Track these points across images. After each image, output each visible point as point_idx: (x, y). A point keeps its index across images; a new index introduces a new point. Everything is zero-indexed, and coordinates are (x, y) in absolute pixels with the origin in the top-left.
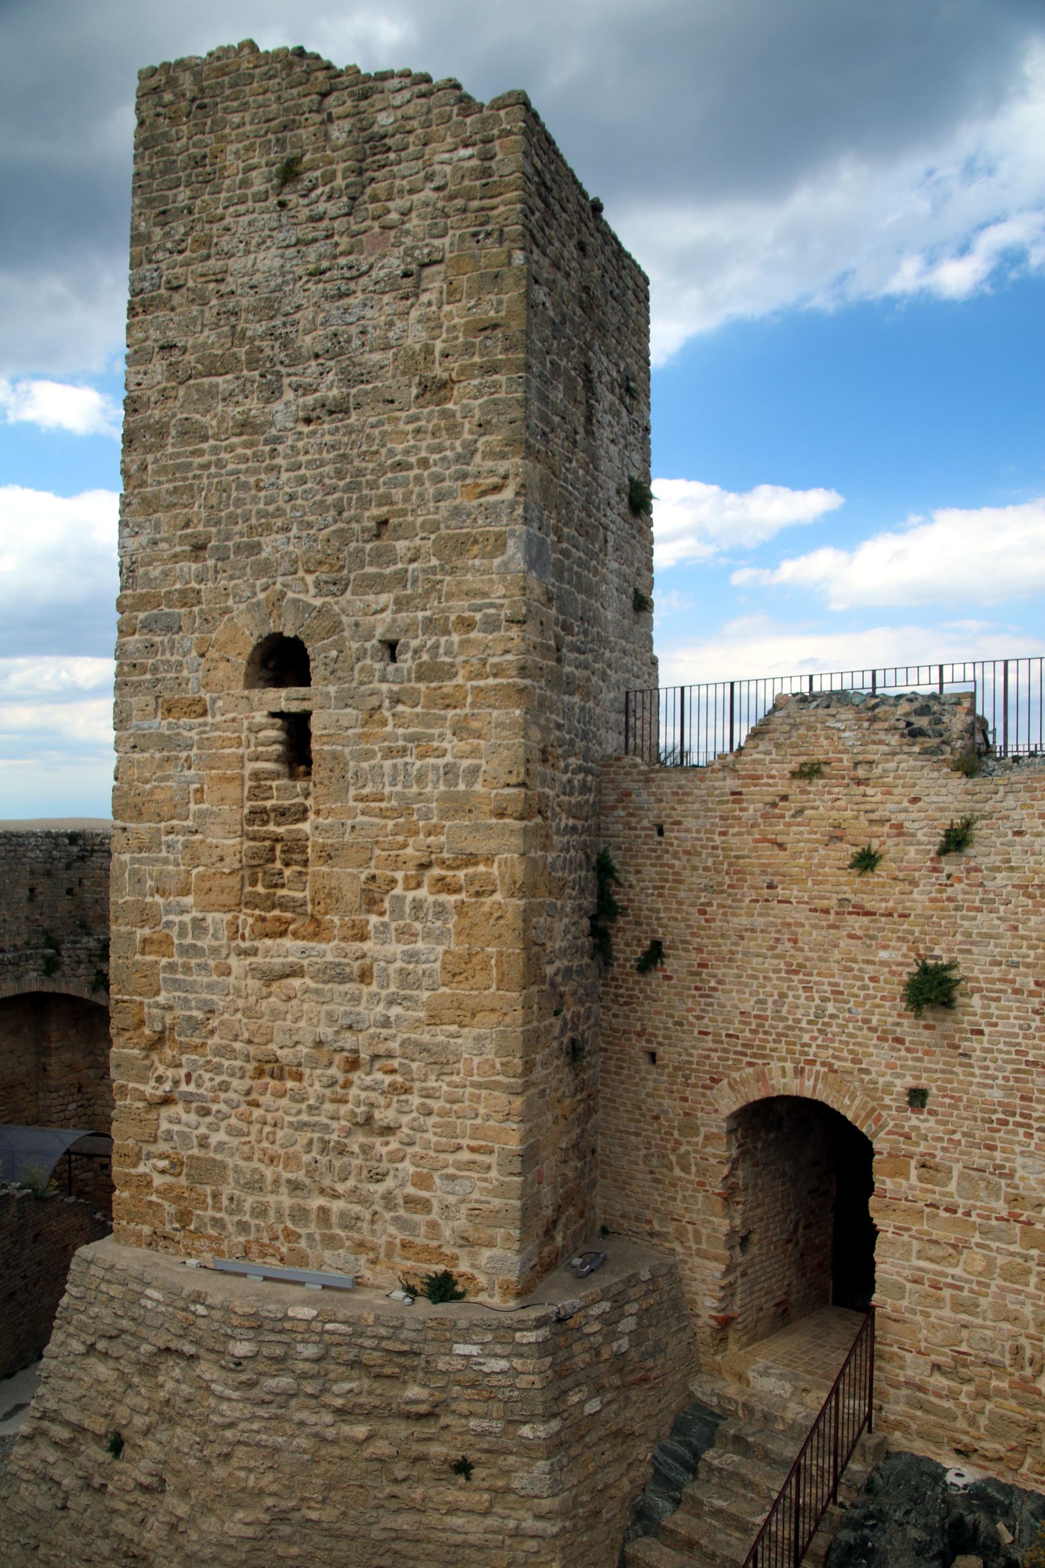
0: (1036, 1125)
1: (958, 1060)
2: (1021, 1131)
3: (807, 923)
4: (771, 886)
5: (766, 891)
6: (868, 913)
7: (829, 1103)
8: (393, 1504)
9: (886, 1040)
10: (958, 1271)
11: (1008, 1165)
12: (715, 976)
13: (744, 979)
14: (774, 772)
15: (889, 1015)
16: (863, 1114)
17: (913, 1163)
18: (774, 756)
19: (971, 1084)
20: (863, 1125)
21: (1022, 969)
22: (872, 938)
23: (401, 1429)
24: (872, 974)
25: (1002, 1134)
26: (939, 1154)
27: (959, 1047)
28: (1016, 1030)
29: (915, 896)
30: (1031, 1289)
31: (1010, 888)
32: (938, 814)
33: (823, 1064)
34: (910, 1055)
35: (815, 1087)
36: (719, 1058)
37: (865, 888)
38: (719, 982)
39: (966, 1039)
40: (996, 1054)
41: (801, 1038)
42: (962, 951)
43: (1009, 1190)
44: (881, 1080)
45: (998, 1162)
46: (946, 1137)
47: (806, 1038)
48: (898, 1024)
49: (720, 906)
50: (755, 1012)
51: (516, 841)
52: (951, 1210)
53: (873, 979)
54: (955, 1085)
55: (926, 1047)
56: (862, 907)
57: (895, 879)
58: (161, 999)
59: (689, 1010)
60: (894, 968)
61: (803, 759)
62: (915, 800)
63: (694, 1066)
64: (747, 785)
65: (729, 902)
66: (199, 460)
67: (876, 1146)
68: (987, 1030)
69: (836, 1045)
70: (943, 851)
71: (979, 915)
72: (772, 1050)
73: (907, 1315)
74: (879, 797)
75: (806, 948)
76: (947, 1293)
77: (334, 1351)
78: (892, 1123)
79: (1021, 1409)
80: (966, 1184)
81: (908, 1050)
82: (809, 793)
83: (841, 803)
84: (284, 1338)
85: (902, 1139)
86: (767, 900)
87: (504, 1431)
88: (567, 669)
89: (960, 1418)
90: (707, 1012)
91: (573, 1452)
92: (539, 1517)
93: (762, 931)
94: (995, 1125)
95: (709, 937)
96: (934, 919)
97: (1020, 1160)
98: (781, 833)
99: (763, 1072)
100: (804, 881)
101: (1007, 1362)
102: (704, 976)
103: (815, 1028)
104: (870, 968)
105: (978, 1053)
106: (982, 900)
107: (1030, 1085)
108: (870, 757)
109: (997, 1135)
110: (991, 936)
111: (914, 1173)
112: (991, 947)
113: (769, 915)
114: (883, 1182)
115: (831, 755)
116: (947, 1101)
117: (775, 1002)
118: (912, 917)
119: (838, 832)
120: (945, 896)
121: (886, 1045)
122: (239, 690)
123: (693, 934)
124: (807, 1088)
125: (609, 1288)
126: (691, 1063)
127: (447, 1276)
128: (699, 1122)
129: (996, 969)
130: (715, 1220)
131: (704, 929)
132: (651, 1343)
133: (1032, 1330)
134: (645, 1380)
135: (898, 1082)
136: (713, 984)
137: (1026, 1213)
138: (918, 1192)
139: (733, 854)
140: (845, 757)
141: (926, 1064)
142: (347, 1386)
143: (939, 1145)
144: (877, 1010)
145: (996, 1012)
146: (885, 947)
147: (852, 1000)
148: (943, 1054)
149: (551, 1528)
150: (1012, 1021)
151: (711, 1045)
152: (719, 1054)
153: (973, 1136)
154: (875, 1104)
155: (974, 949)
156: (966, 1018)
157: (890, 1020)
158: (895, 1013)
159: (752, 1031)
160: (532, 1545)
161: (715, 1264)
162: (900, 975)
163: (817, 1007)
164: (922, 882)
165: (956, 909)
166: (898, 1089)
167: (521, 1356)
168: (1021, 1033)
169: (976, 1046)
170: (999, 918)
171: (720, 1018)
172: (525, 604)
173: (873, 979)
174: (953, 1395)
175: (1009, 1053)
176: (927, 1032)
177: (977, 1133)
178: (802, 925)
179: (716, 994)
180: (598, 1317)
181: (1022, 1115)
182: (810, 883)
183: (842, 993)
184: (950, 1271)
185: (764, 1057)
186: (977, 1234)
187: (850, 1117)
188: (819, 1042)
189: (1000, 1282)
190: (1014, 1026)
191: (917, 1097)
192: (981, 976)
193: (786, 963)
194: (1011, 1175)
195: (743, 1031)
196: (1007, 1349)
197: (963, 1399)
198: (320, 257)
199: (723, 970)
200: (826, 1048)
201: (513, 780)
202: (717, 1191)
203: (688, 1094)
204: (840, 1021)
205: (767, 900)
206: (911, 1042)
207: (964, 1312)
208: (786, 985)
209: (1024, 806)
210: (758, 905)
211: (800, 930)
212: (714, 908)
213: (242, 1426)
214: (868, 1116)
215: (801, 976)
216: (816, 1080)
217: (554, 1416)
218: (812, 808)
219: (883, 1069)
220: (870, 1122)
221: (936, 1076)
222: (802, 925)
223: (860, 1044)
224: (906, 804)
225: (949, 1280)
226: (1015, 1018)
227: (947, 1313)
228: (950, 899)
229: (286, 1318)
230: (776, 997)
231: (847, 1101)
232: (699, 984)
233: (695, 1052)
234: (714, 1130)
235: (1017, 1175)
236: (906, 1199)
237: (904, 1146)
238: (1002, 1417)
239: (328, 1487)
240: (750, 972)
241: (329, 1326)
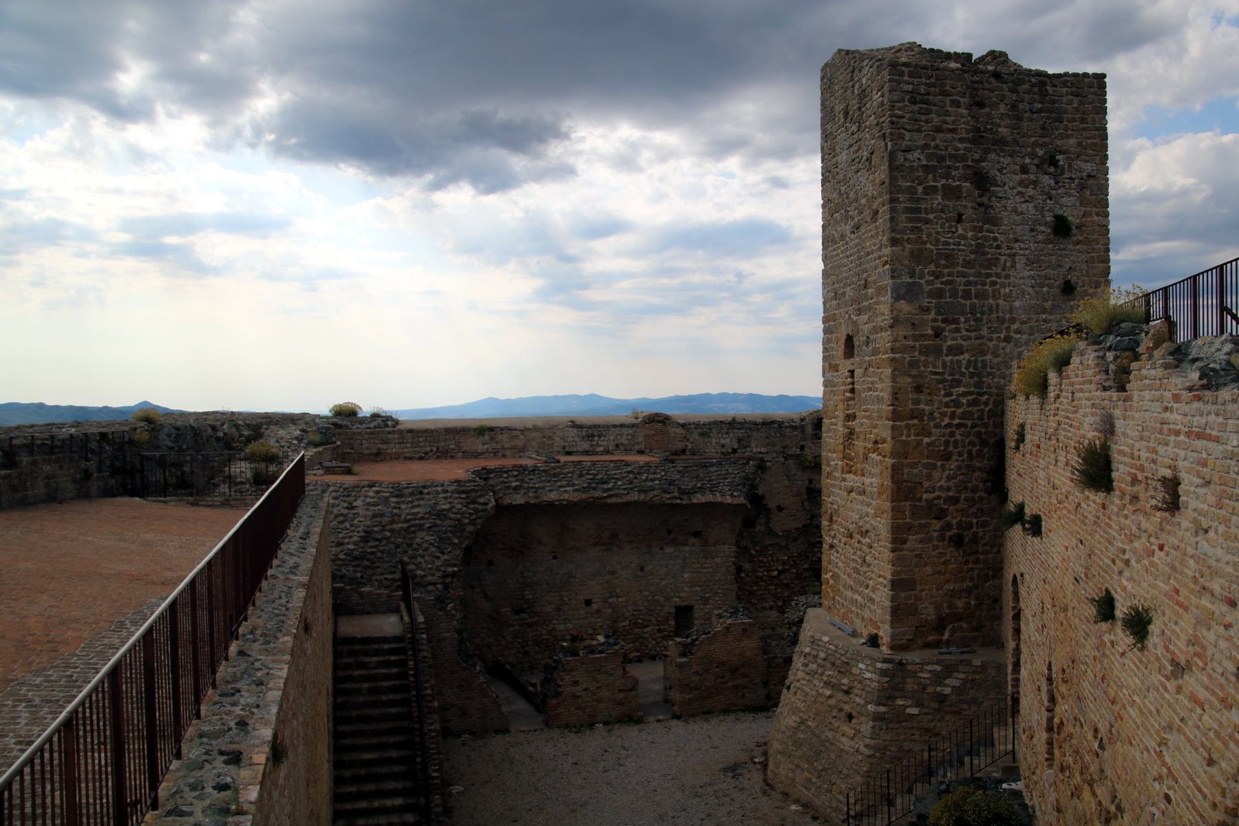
8: (830, 726)
23: (840, 695)
51: (890, 432)
58: (830, 500)
66: (835, 253)
77: (830, 657)
84: (818, 648)
87: (864, 705)
88: (950, 342)
91: (891, 725)
92: (865, 746)
122: (842, 361)
125: (943, 661)
127: (876, 635)
132: (969, 697)
134: (960, 714)
142: (829, 673)
149: (867, 752)
160: (860, 757)
167: (875, 673)
172: (892, 318)
180: (930, 671)
198: (854, 153)
201: (890, 403)
213: (801, 681)
217: (885, 705)
229: (820, 640)
239: (816, 714)
241: (831, 646)
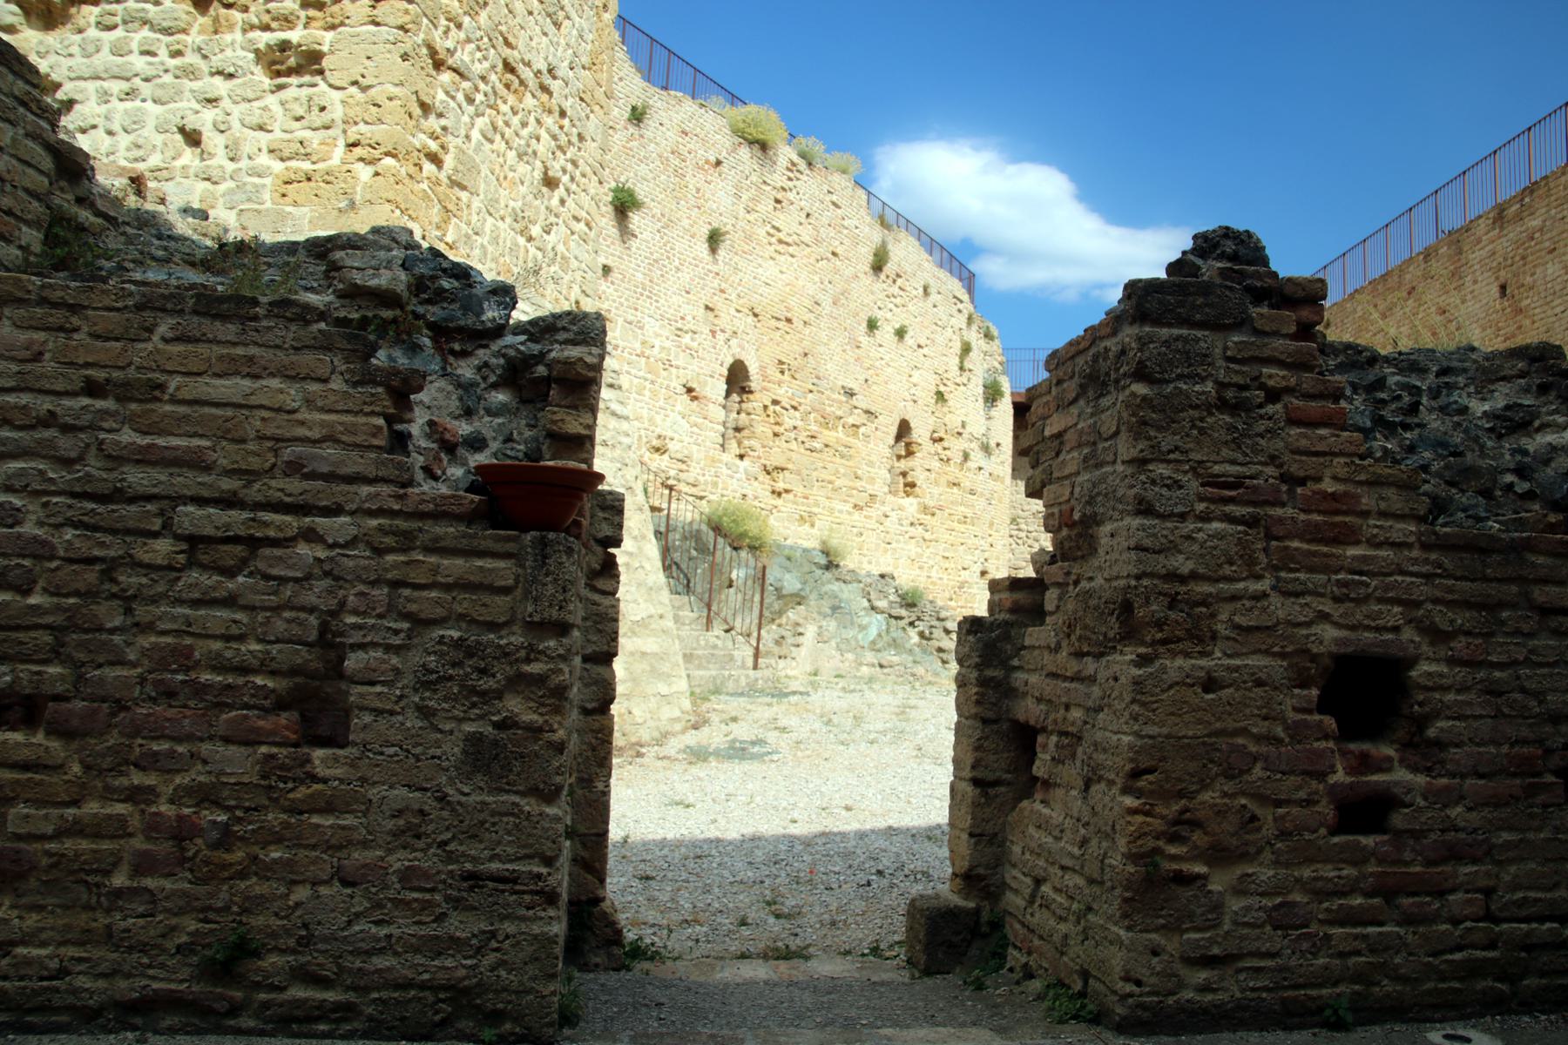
26: (614, 310)
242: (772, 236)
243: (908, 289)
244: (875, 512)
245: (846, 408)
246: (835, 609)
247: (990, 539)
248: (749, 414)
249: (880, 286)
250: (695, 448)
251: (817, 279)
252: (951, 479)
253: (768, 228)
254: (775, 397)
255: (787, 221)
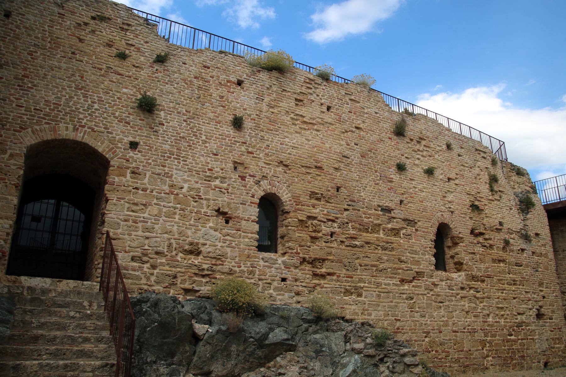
0: (182, 159)
1: (152, 133)
2: (176, 161)
3: (89, 72)
4: (73, 53)
5: (70, 55)
6: (120, 74)
7: (90, 144)
9: (122, 122)
10: (146, 215)
11: (170, 173)
12: (33, 82)
13: (50, 87)
14: (83, 13)
15: (124, 113)
16: (107, 150)
17: (129, 171)
18: (84, 8)
19: (157, 142)
20: (106, 154)
21: (181, 106)
22: (120, 83)
24: (119, 96)
25: (168, 161)
26: (141, 167)
27: (154, 129)
28: (177, 125)
29: (141, 73)
30: (177, 220)
31: (179, 79)
32: (155, 50)
33: (89, 128)
34: (132, 129)
35: (83, 137)
36: (27, 118)
37: (120, 66)
38: (35, 86)
39: (157, 126)
40: (168, 133)
41: (79, 116)
42: (158, 96)
43: (170, 182)
44: (117, 137)
45: (166, 171)
46: (145, 161)
47: (81, 116)
48: (128, 117)
49: (41, 54)
50: (54, 102)
52: (144, 190)
53: (118, 98)
54: (151, 142)
55: (139, 127)
56: (118, 72)
57: (134, 66)
59: (10, 95)
60: (129, 96)
61: (99, 14)
62: (147, 42)
63: (10, 120)
64: (68, 13)
65: (48, 54)
67: (112, 163)
68: (166, 124)
69: (97, 121)
70: (155, 62)
71: (167, 85)
72: (61, 118)
73: (120, 236)
74: (132, 37)
75: (88, 81)
76: (140, 225)
78: (121, 154)
79: (170, 269)
80: (152, 180)
81: (131, 127)
82: (100, 26)
83: (115, 34)
85: (125, 161)
86: (70, 58)
89: (143, 279)
90: (24, 97)
93: (65, 70)
94: (166, 158)
95: (32, 65)
96: (149, 82)
97: (175, 171)
98: (83, 35)
99: (54, 128)
100: (92, 56)
101: (165, 250)
102: (25, 81)
103: (87, 113)
104: (118, 94)
105: (161, 131)
106: (168, 81)
107: (181, 145)
108: (131, 23)
109: (166, 162)
110: (171, 93)
111: (128, 175)
112: (170, 97)
113: (70, 64)
114: (114, 178)
115: (112, 17)
116: (147, 147)
117: (66, 99)
118: (139, 80)
119: (111, 43)
120: (154, 76)
121: (121, 124)
123: (23, 62)
124: (79, 137)
126: (9, 118)
128: (8, 147)
129: (171, 104)
130: (9, 197)
131: (30, 61)
133: (176, 236)
135: (125, 138)
136: (30, 85)
137: (176, 191)
138: (130, 183)
139: (55, 36)
140: (119, 19)
141: (139, 133)
143: (142, 164)
144: (119, 110)
145: (170, 119)
146: (126, 88)
147: (107, 105)
148: (147, 130)
150: (175, 122)
151: (23, 112)
152: (28, 117)
153: (157, 162)
154: (113, 146)
155: (164, 96)
156: (157, 119)
157: (124, 115)
158: (127, 113)
159: (50, 109)
161: (6, 221)
162: (132, 99)
163: (89, 105)
164: (145, 69)
165: (158, 81)
166: (126, 141)
168: (178, 127)
169: (161, 129)
170: (174, 88)
171: (31, 101)
173: (118, 98)
174: (141, 268)
175: (173, 133)
176: (141, 122)
177: (159, 160)
178: (88, 72)
179: (32, 90)
181: (177, 155)
182: (94, 57)
183: (103, 101)
184: (142, 215)
185: (57, 121)
186: (155, 200)
187: (100, 150)
188: (88, 118)
189: (164, 218)
190: (176, 124)
191: (134, 145)
192: (166, 105)
193: (75, 84)
194: (171, 176)
195: (46, 109)
196: (166, 245)
197: (145, 269)
199: (38, 81)
200: (92, 121)
202: (13, 183)
203: (2, 133)
204: (100, 112)
205: (70, 58)
206: (133, 124)
207: (148, 232)
208: (74, 93)
209: (187, 56)
210: (64, 59)
211: (85, 74)
212: (39, 54)
214: (110, 150)
215: (83, 91)
216: (84, 134)
218: (101, 32)
219: (119, 132)
220: (111, 153)
221: (143, 138)
222: (88, 72)
223: (109, 122)
224: (142, 42)
225: (142, 219)
226: (177, 122)
227: (140, 233)
228: (156, 77)
230: (67, 97)
231: (99, 144)
232: (21, 84)
233: (12, 114)
234: (18, 152)
235: (174, 177)
236: (124, 186)
237: (125, 164)
238: (162, 274)
240: (54, 84)
242: (297, 120)
243: (432, 146)
244: (422, 282)
245: (385, 218)
246: (318, 352)
247: (542, 293)
248: (287, 226)
249: (402, 144)
250: (229, 250)
251: (343, 143)
252: (495, 257)
253: (292, 115)
254: (309, 214)
255: (308, 112)
